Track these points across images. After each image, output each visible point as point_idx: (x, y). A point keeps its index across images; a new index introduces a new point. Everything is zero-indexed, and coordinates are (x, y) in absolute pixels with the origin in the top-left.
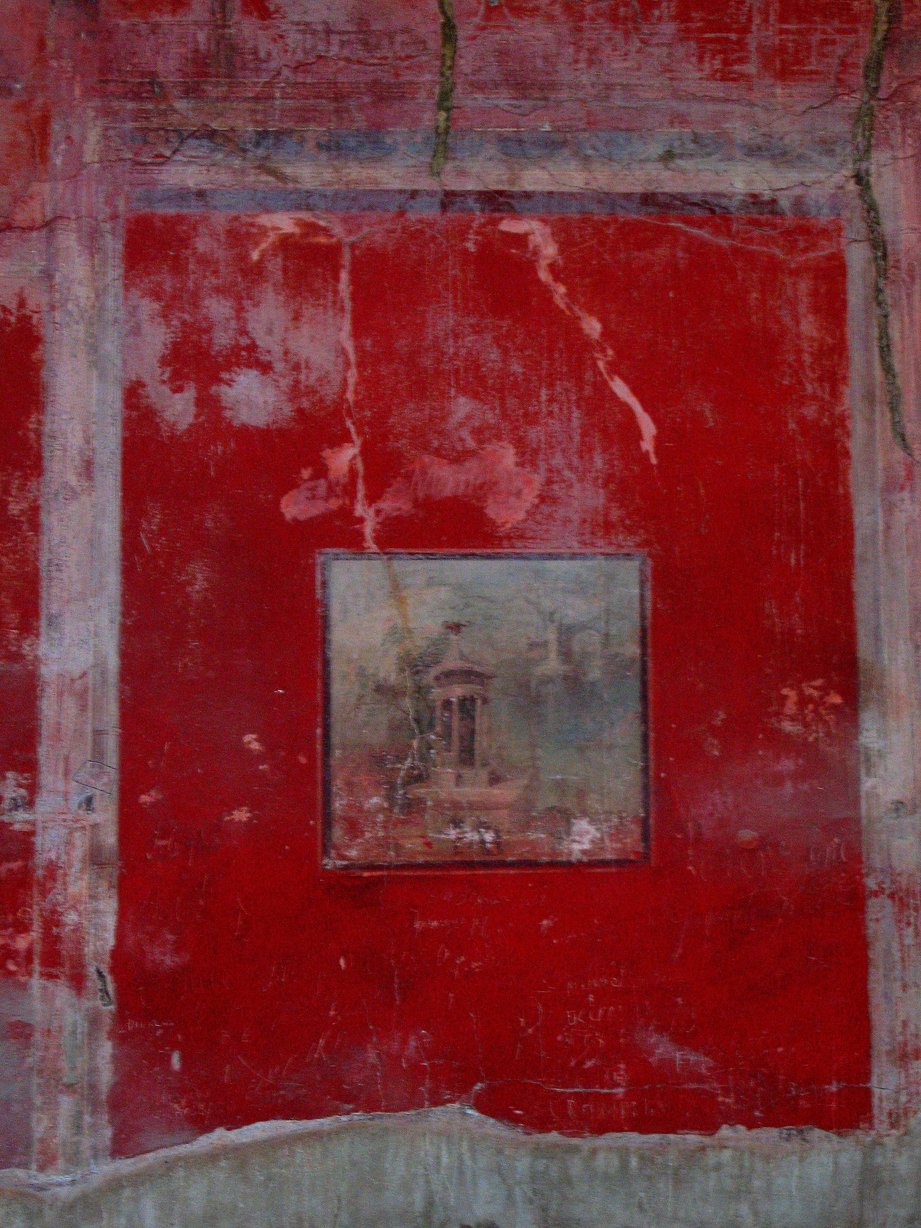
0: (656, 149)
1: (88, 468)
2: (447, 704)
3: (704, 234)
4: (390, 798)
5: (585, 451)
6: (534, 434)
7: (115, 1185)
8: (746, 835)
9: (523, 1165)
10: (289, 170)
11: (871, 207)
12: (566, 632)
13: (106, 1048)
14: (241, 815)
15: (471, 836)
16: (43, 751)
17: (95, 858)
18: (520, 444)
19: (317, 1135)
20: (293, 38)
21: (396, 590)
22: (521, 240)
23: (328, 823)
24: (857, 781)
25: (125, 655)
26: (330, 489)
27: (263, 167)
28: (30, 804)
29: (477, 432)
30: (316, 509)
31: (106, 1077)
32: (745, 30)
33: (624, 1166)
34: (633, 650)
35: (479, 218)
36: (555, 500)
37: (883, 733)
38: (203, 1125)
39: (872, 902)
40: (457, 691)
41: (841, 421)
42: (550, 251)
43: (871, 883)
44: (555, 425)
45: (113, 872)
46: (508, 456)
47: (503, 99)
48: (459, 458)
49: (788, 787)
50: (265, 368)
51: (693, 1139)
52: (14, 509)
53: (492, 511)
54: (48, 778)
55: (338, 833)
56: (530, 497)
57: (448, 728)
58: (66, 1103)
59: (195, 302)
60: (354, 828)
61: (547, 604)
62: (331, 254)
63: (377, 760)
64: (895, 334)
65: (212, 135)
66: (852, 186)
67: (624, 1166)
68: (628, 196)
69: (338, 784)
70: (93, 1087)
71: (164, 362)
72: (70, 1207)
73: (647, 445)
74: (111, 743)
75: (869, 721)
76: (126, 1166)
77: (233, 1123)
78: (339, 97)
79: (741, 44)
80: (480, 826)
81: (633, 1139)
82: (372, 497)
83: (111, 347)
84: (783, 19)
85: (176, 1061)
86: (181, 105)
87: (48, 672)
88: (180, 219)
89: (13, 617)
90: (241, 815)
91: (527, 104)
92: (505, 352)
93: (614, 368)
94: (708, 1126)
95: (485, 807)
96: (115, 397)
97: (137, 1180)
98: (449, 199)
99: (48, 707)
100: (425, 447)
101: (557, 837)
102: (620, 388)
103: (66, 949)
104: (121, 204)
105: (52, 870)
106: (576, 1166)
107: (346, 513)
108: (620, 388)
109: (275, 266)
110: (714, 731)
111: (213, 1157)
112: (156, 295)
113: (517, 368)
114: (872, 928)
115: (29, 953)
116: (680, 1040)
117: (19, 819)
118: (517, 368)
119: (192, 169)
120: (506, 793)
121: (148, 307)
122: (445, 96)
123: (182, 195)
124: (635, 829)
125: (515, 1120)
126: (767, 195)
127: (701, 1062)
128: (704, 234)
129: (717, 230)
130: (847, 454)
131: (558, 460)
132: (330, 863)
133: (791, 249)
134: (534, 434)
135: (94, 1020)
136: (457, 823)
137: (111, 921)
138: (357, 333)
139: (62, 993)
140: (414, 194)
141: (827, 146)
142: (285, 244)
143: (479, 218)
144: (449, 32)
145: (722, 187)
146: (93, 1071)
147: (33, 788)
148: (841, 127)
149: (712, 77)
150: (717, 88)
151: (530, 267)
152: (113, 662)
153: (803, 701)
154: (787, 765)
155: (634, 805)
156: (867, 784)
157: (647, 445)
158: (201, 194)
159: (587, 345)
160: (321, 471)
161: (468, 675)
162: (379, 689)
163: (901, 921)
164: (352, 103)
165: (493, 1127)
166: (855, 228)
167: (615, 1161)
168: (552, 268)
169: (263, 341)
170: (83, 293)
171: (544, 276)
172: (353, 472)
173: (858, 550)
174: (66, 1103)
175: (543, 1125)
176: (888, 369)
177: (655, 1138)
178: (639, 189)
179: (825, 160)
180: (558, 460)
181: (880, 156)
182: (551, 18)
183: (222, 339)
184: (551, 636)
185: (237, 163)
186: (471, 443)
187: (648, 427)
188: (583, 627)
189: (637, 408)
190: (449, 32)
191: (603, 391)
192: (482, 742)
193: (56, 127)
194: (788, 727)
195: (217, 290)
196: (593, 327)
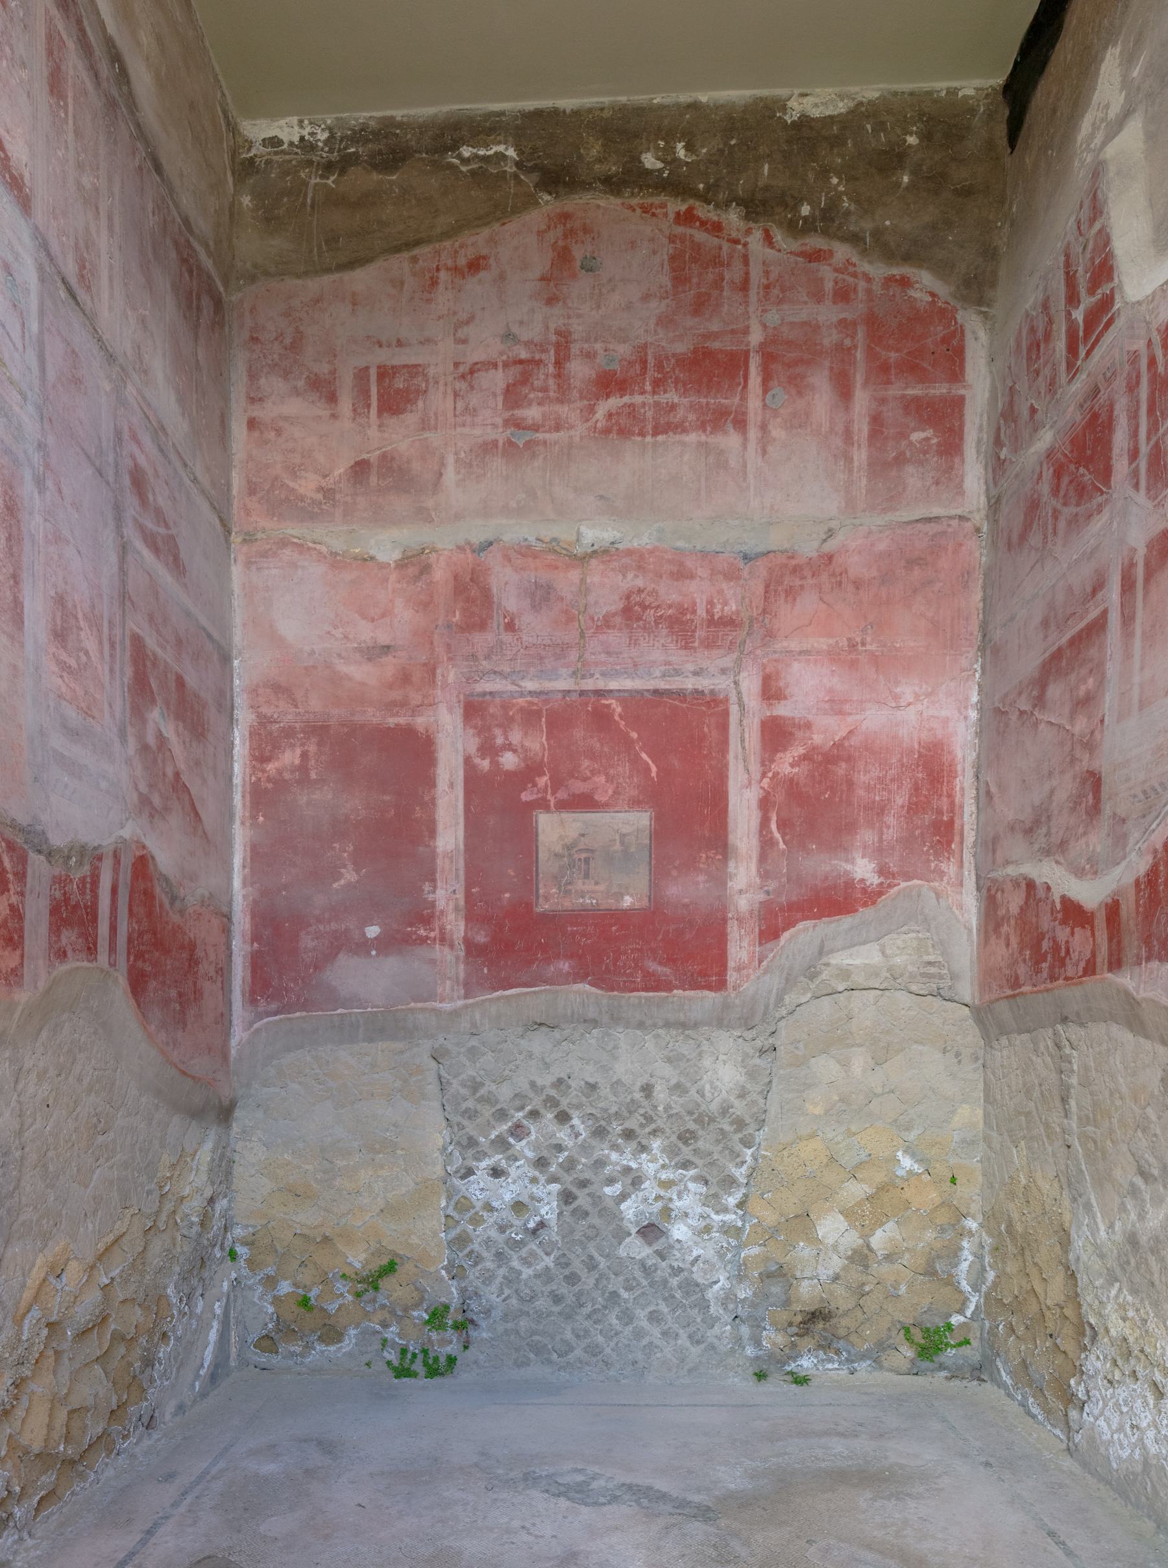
0: (658, 673)
1: (452, 785)
2: (580, 860)
3: (676, 703)
4: (559, 889)
5: (631, 777)
6: (612, 772)
7: (466, 1007)
8: (686, 900)
9: (605, 1001)
10: (523, 684)
11: (739, 693)
12: (623, 836)
13: (462, 967)
14: (507, 895)
15: (588, 901)
16: (438, 875)
17: (457, 909)
18: (607, 775)
19: (534, 992)
20: (525, 638)
21: (562, 822)
22: (608, 706)
23: (537, 898)
24: (726, 884)
25: (466, 845)
26: (538, 791)
27: (513, 683)
28: (434, 892)
29: (592, 771)
30: (535, 797)
31: (462, 975)
32: (694, 631)
33: (640, 1002)
34: (647, 841)
35: (593, 699)
36: (620, 794)
37: (736, 868)
38: (495, 989)
39: (730, 922)
40: (583, 856)
41: (726, 766)
42: (619, 710)
43: (730, 915)
44: (620, 769)
45: (463, 913)
46: (601, 779)
47: (603, 657)
48: (585, 779)
49: (701, 886)
50: (515, 751)
51: (664, 994)
52: (426, 799)
53: (596, 797)
54: (439, 884)
55: (541, 900)
56: (610, 792)
57: (580, 867)
58: (448, 982)
59: (489, 729)
60: (547, 899)
61: (616, 827)
62: (538, 713)
63: (556, 878)
64: (747, 736)
65: (495, 672)
66: (732, 685)
67: (640, 1002)
68: (648, 691)
69: (541, 885)
70: (457, 978)
71: (478, 750)
72: (451, 1013)
73: (654, 774)
74: (462, 873)
75: (732, 864)
76: (471, 1001)
77: (505, 989)
78: (541, 658)
79: (693, 636)
80: (591, 898)
81: (644, 994)
82: (553, 793)
83: (460, 746)
84: (708, 627)
85: (486, 971)
86: (484, 663)
87: (440, 850)
88: (483, 702)
89: (426, 833)
90: (507, 895)
91: (611, 660)
92: (602, 745)
93: (642, 749)
94: (670, 990)
95: (593, 892)
96: (461, 760)
97: (472, 1005)
98: (582, 693)
99: (439, 862)
100: (573, 777)
101: (618, 901)
102: (644, 756)
103: (447, 937)
104: (462, 697)
105: (442, 912)
106: (623, 1002)
107: (544, 799)
108: (644, 756)
109: (518, 717)
110: (675, 868)
111: (499, 998)
112: (476, 728)
113: (606, 749)
114: (729, 930)
115: (435, 939)
116: (660, 963)
117: (431, 897)
118: (606, 749)
119: (488, 685)
120: (601, 888)
121: (471, 731)
122: (580, 657)
123: (484, 694)
124: (646, 900)
125: (602, 988)
126: (700, 688)
127: (667, 970)
128: (676, 703)
129: (681, 701)
130: (727, 777)
131: (621, 780)
132: (539, 910)
133: (709, 707)
134: (612, 772)
135: (457, 958)
136: (583, 897)
137: (462, 928)
138: (547, 740)
139: (446, 950)
140: (569, 691)
141: (723, 671)
142: (522, 709)
143: (593, 699)
144: (582, 635)
145: (684, 687)
146: (457, 974)
147: (435, 887)
148: (731, 665)
149: (681, 648)
150: (683, 652)
151: (613, 715)
152: (462, 847)
153: (707, 857)
154: (701, 878)
155: (646, 891)
156: (730, 884)
157: (654, 774)
158: (491, 693)
159: (633, 741)
160: (535, 785)
161: (587, 850)
162: (556, 855)
163: (740, 926)
164: (546, 661)
165: (594, 990)
166: (733, 698)
167: (637, 1001)
168: (620, 715)
169: (514, 742)
170: (449, 728)
171: (617, 718)
172: (546, 786)
173: (730, 807)
174: (448, 982)
175: (612, 990)
176: (744, 748)
177: (651, 994)
178: (651, 688)
179: (724, 677)
180: (621, 780)
181: (744, 674)
182: (620, 629)
183: (500, 741)
184: (617, 837)
185: (504, 682)
186: (589, 774)
187: (654, 769)
188: (629, 834)
189: (650, 762)
190: (582, 635)
191: (637, 755)
192: (592, 871)
193: (439, 671)
194: (702, 866)
195: (499, 726)
196: (634, 735)
